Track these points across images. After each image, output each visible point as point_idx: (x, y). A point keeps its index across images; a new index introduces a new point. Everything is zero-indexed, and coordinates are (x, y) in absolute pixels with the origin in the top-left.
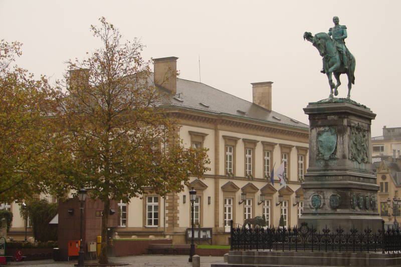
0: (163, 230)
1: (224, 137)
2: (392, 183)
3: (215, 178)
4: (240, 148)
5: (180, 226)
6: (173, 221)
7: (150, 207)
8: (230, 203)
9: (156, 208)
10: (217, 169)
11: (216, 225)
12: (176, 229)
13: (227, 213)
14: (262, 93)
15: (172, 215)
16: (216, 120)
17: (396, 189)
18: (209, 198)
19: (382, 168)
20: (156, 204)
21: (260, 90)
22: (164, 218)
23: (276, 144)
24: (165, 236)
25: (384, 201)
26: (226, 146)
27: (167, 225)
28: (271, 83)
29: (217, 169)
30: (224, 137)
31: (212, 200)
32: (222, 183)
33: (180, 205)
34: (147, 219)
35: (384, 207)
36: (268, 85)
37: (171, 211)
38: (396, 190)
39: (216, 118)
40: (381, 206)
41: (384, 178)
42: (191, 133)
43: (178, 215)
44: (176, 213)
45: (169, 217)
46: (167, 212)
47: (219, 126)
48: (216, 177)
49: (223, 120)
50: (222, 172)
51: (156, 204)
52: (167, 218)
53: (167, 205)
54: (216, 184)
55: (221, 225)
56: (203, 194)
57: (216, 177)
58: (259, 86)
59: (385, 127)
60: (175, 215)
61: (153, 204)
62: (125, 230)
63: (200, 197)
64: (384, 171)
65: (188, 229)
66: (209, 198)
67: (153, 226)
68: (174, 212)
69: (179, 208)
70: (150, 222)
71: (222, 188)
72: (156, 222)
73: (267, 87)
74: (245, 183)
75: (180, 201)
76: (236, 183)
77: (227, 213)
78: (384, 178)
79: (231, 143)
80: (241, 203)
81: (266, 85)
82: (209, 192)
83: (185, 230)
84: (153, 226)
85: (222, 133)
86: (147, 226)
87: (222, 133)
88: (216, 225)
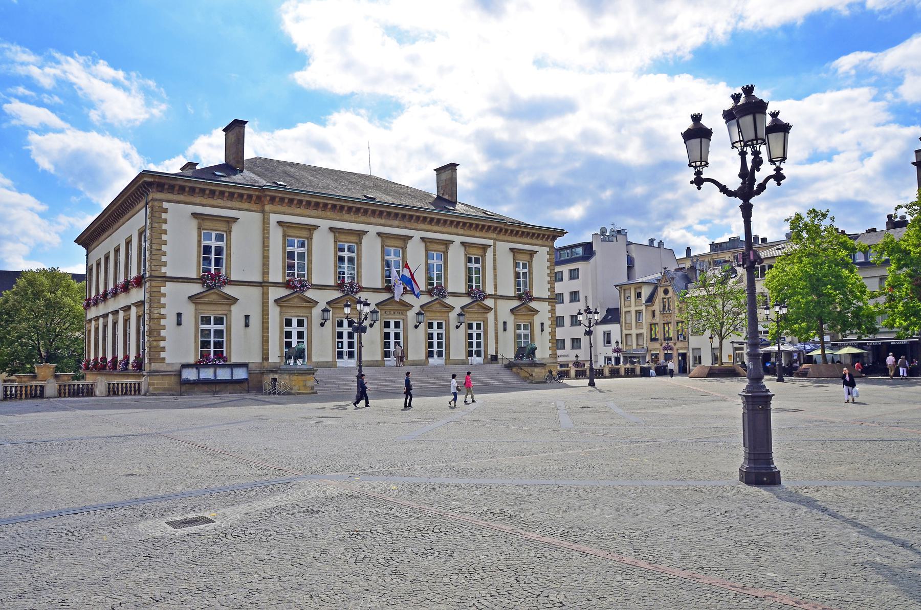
1: (280, 223)
11: (265, 358)
12: (155, 366)
21: (445, 175)
29: (265, 272)
31: (255, 321)
32: (275, 293)
41: (666, 292)
47: (268, 207)
48: (264, 285)
50: (276, 274)
57: (264, 285)
65: (185, 366)
75: (169, 322)
78: (666, 292)
83: (178, 367)
85: (274, 218)
87: (274, 218)
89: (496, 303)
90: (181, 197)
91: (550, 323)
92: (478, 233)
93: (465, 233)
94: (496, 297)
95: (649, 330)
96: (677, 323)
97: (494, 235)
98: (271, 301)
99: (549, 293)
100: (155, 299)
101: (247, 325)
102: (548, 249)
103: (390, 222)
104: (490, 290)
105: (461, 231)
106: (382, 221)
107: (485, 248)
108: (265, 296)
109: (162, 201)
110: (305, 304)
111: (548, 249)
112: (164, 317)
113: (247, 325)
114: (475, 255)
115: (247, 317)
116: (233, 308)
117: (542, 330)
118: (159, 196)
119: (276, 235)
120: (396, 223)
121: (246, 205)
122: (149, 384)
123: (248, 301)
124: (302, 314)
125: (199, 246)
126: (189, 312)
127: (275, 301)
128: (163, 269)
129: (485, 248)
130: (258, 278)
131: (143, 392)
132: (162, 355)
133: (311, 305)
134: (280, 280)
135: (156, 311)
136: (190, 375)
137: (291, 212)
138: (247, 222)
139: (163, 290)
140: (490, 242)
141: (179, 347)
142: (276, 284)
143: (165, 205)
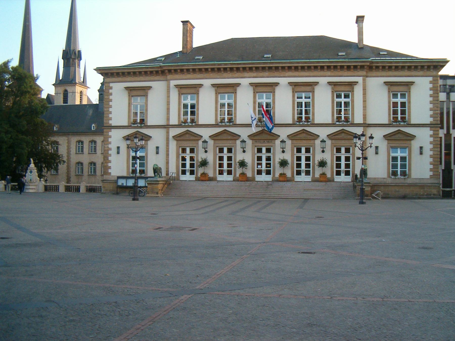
1: (177, 86)
12: (106, 177)
18: (157, 148)
26: (180, 94)
29: (168, 119)
32: (174, 132)
48: (167, 127)
65: (119, 178)
75: (113, 152)
85: (173, 83)
90: (120, 79)
91: (431, 146)
92: (346, 73)
93: (333, 74)
94: (366, 125)
97: (364, 73)
98: (171, 137)
99: (431, 119)
101: (157, 153)
102: (431, 79)
103: (261, 74)
104: (358, 119)
105: (329, 73)
106: (255, 74)
107: (352, 84)
108: (168, 133)
109: (109, 83)
110: (194, 138)
111: (431, 79)
112: (110, 149)
113: (157, 153)
114: (342, 91)
115: (157, 148)
116: (149, 142)
119: (174, 94)
120: (267, 74)
121: (157, 78)
123: (157, 138)
124: (230, 144)
125: (254, 102)
126: (123, 146)
127: (173, 137)
128: (110, 122)
129: (352, 84)
130: (163, 123)
132: (110, 171)
134: (176, 123)
135: (106, 146)
136: (121, 182)
137: (185, 77)
138: (158, 87)
139: (110, 134)
140: (360, 80)
141: (119, 166)
143: (111, 85)
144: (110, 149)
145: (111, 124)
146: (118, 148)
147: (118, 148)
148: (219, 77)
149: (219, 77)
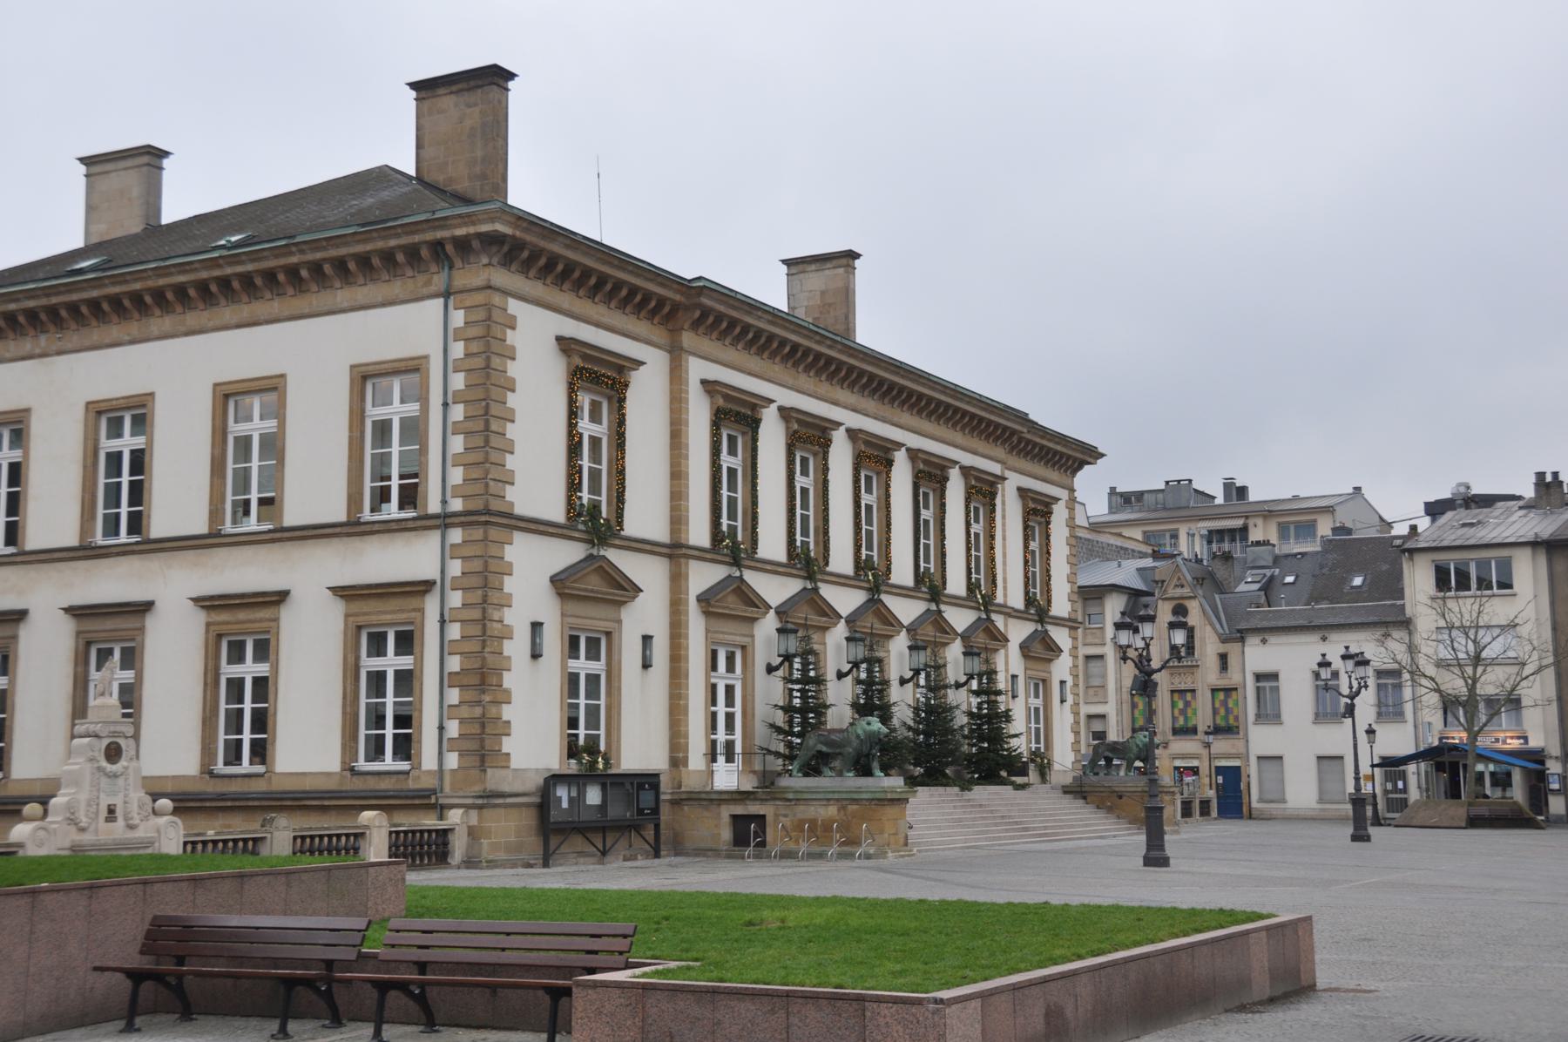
0: (428, 783)
2: (1208, 628)
3: (670, 556)
4: (772, 437)
5: (515, 763)
6: (482, 740)
7: (377, 679)
8: (730, 668)
9: (406, 680)
10: (678, 519)
11: (677, 760)
12: (496, 779)
13: (721, 709)
14: (823, 293)
15: (478, 711)
16: (676, 308)
17: (1222, 648)
18: (647, 640)
19: (1175, 581)
20: (406, 662)
21: (816, 280)
22: (441, 728)
23: (899, 445)
24: (441, 810)
25: (1183, 687)
27: (452, 761)
28: (852, 255)
29: (678, 519)
30: (709, 386)
32: (702, 577)
33: (514, 664)
34: (363, 732)
35: (1181, 705)
36: (844, 261)
37: (471, 695)
38: (1221, 651)
39: (678, 297)
40: (1173, 705)
42: (566, 345)
43: (507, 712)
44: (498, 703)
45: (462, 721)
46: (454, 696)
47: (688, 339)
48: (675, 552)
49: (706, 312)
50: (699, 533)
51: (406, 662)
52: (453, 729)
53: (454, 663)
54: (677, 580)
55: (696, 759)
56: (619, 622)
57: (675, 552)
58: (813, 267)
59: (1113, 490)
60: (492, 711)
61: (391, 662)
62: (259, 786)
63: (608, 634)
64: (1179, 592)
65: (555, 779)
66: (647, 640)
67: (389, 763)
68: (487, 698)
69: (508, 680)
70: (376, 750)
71: (700, 599)
72: (405, 747)
73: (841, 270)
74: (792, 587)
75: (516, 648)
76: (754, 579)
77: (721, 709)
79: (736, 416)
80: (777, 668)
81: (835, 262)
82: (646, 614)
83: (541, 781)
84: (389, 763)
85: (698, 369)
86: (362, 765)
87: (698, 369)
88: (677, 760)
89: (1006, 625)
94: (1011, 613)
95: (1127, 707)
96: (1213, 691)
97: (1000, 452)
100: (485, 583)
101: (646, 665)
117: (1063, 701)
118: (501, 277)
122: (473, 833)
127: (701, 599)
128: (511, 494)
131: (457, 855)
133: (750, 612)
142: (700, 554)
143: (514, 306)
144: (507, 634)
145: (512, 504)
146: (536, 627)
147: (536, 627)
148: (791, 382)
149: (791, 382)
